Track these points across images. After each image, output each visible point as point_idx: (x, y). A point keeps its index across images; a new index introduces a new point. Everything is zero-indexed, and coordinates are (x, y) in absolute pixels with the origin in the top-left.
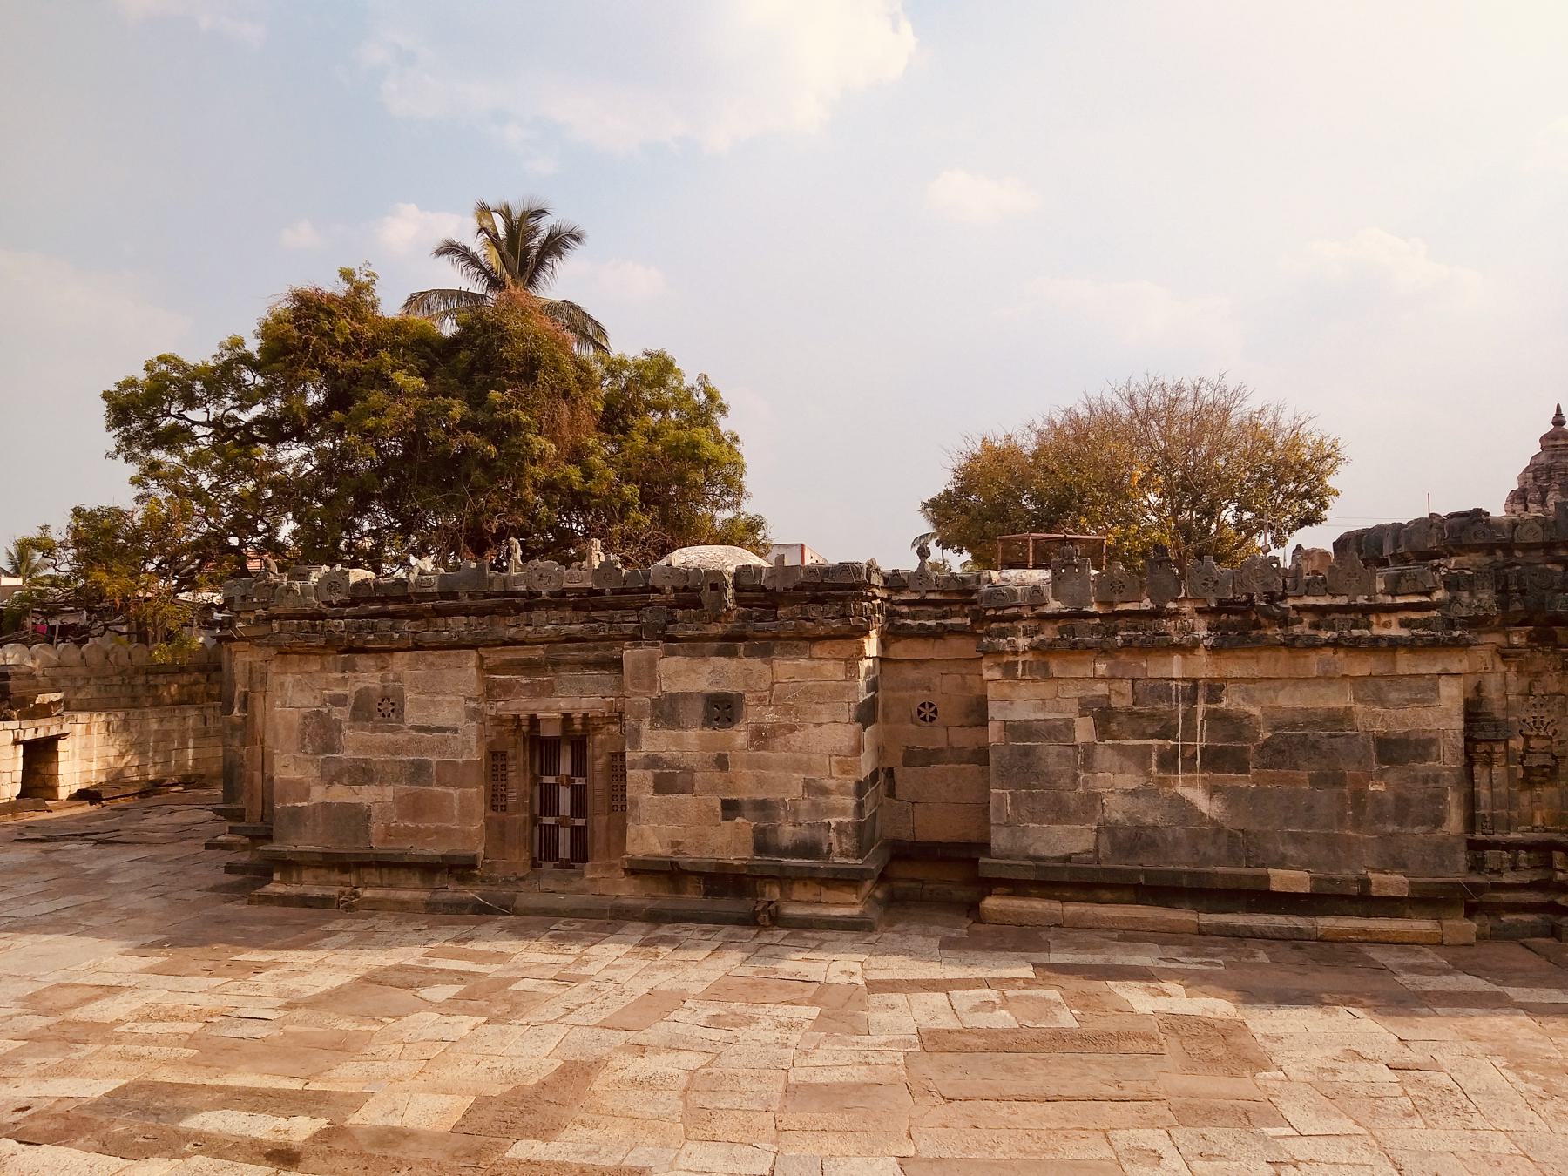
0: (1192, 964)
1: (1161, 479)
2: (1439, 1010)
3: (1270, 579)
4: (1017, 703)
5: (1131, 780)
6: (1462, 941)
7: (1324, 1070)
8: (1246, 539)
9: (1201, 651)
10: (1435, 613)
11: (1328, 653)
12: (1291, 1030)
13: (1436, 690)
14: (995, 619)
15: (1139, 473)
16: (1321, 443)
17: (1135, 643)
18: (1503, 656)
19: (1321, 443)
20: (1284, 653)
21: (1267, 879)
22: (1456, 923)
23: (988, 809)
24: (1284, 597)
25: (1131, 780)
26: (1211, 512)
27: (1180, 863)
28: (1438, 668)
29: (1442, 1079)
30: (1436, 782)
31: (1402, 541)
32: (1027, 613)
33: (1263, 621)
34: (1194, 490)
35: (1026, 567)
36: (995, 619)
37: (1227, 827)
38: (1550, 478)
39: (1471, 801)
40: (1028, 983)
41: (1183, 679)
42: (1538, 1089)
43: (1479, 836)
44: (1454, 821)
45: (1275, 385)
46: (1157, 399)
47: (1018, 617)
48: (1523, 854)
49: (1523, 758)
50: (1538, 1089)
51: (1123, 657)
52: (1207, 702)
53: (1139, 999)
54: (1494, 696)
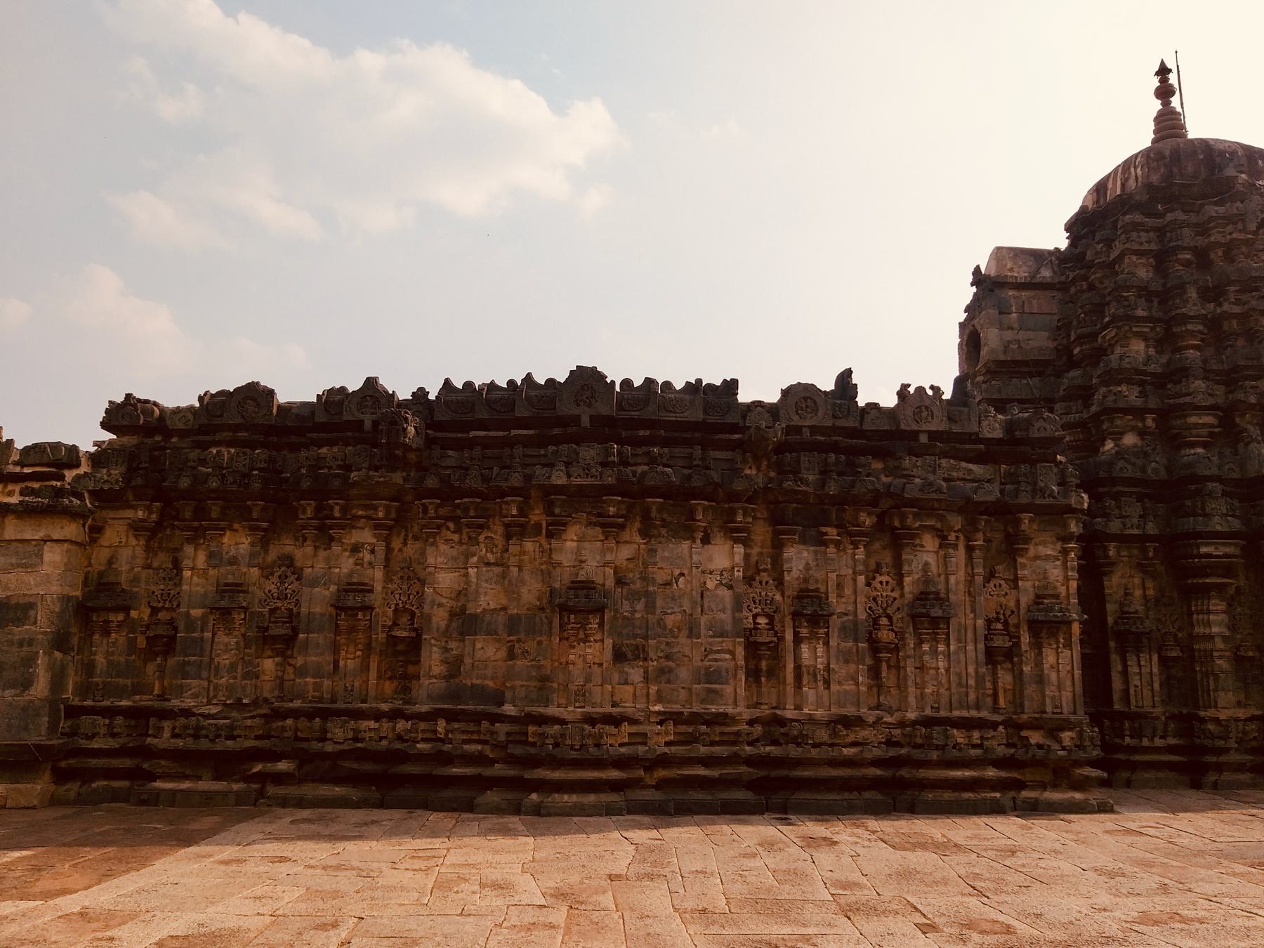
18: (135, 529)
28: (40, 535)
30: (30, 645)
44: (41, 687)
48: (120, 720)
54: (125, 568)
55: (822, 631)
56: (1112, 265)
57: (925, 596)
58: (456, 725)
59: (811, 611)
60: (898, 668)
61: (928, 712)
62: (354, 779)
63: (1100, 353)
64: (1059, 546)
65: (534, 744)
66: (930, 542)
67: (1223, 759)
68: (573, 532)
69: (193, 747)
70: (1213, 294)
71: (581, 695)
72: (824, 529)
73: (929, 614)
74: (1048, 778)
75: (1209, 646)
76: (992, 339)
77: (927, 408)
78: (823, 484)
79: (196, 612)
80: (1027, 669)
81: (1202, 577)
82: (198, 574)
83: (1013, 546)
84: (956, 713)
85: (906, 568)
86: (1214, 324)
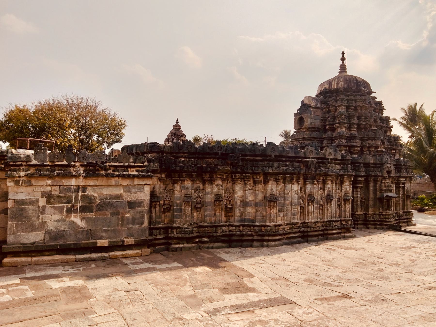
0: (72, 271)
1: (75, 125)
2: (139, 274)
3: (102, 157)
4: (18, 193)
5: (58, 217)
6: (147, 254)
7: (107, 296)
8: (99, 145)
9: (81, 177)
10: (144, 168)
11: (117, 179)
12: (99, 286)
13: (144, 189)
14: (13, 165)
15: (69, 123)
16: (121, 120)
17: (61, 175)
19: (121, 120)
20: (105, 179)
21: (97, 243)
22: (145, 250)
23: (7, 229)
24: (106, 163)
25: (58, 217)
26: (90, 137)
27: (71, 241)
29: (138, 292)
31: (138, 149)
32: (24, 164)
33: (100, 169)
34: (85, 130)
35: (26, 149)
36: (13, 165)
37: (86, 229)
38: (174, 136)
39: (150, 218)
40: (17, 285)
41: (75, 186)
42: (160, 291)
43: (152, 226)
44: (146, 223)
45: (108, 102)
46: (75, 101)
47: (21, 165)
48: (162, 231)
49: (163, 206)
50: (160, 291)
51: (57, 179)
52: (82, 192)
53: (55, 284)
57: (328, 195)
58: (245, 228)
59: (311, 199)
60: (322, 210)
61: (328, 219)
62: (222, 241)
63: (334, 130)
65: (263, 231)
66: (330, 182)
68: (270, 183)
69: (185, 236)
70: (359, 118)
71: (273, 220)
73: (329, 199)
74: (345, 231)
75: (357, 199)
76: (308, 122)
78: (316, 171)
79: (178, 202)
80: (343, 209)
82: (178, 191)
84: (333, 219)
86: (359, 125)
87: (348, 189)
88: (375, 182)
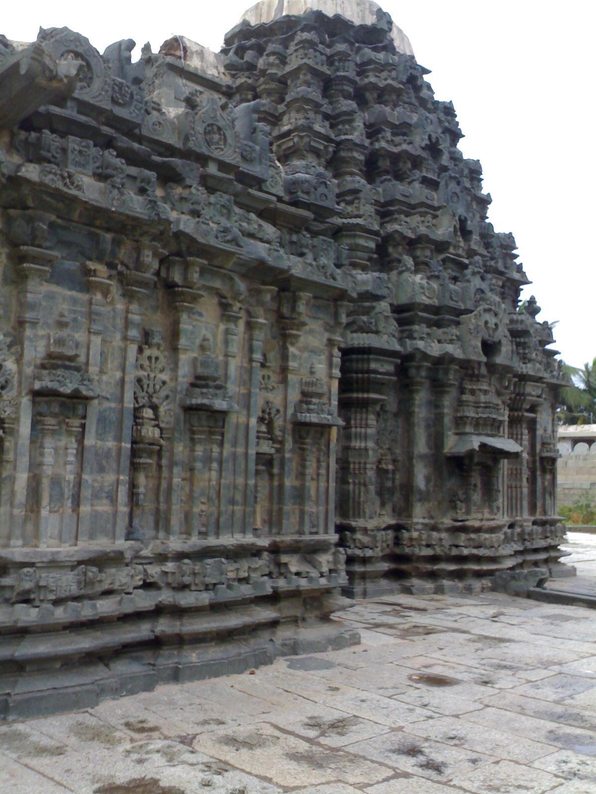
55: (76, 422)
56: (283, 81)
64: (327, 335)
66: (208, 308)
67: (369, 568)
72: (91, 265)
77: (219, 129)
81: (363, 391)
83: (284, 328)
85: (183, 342)
87: (321, 368)
88: (438, 387)
